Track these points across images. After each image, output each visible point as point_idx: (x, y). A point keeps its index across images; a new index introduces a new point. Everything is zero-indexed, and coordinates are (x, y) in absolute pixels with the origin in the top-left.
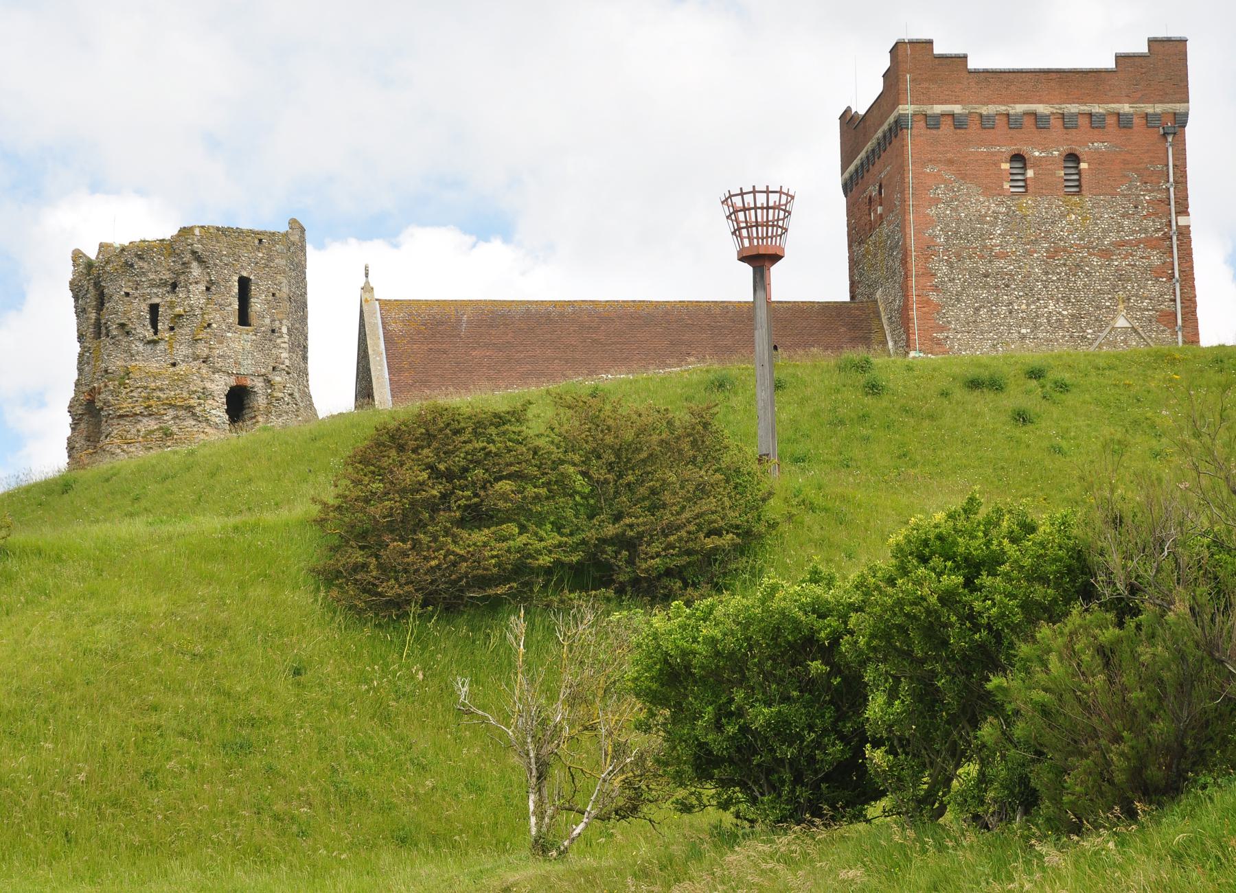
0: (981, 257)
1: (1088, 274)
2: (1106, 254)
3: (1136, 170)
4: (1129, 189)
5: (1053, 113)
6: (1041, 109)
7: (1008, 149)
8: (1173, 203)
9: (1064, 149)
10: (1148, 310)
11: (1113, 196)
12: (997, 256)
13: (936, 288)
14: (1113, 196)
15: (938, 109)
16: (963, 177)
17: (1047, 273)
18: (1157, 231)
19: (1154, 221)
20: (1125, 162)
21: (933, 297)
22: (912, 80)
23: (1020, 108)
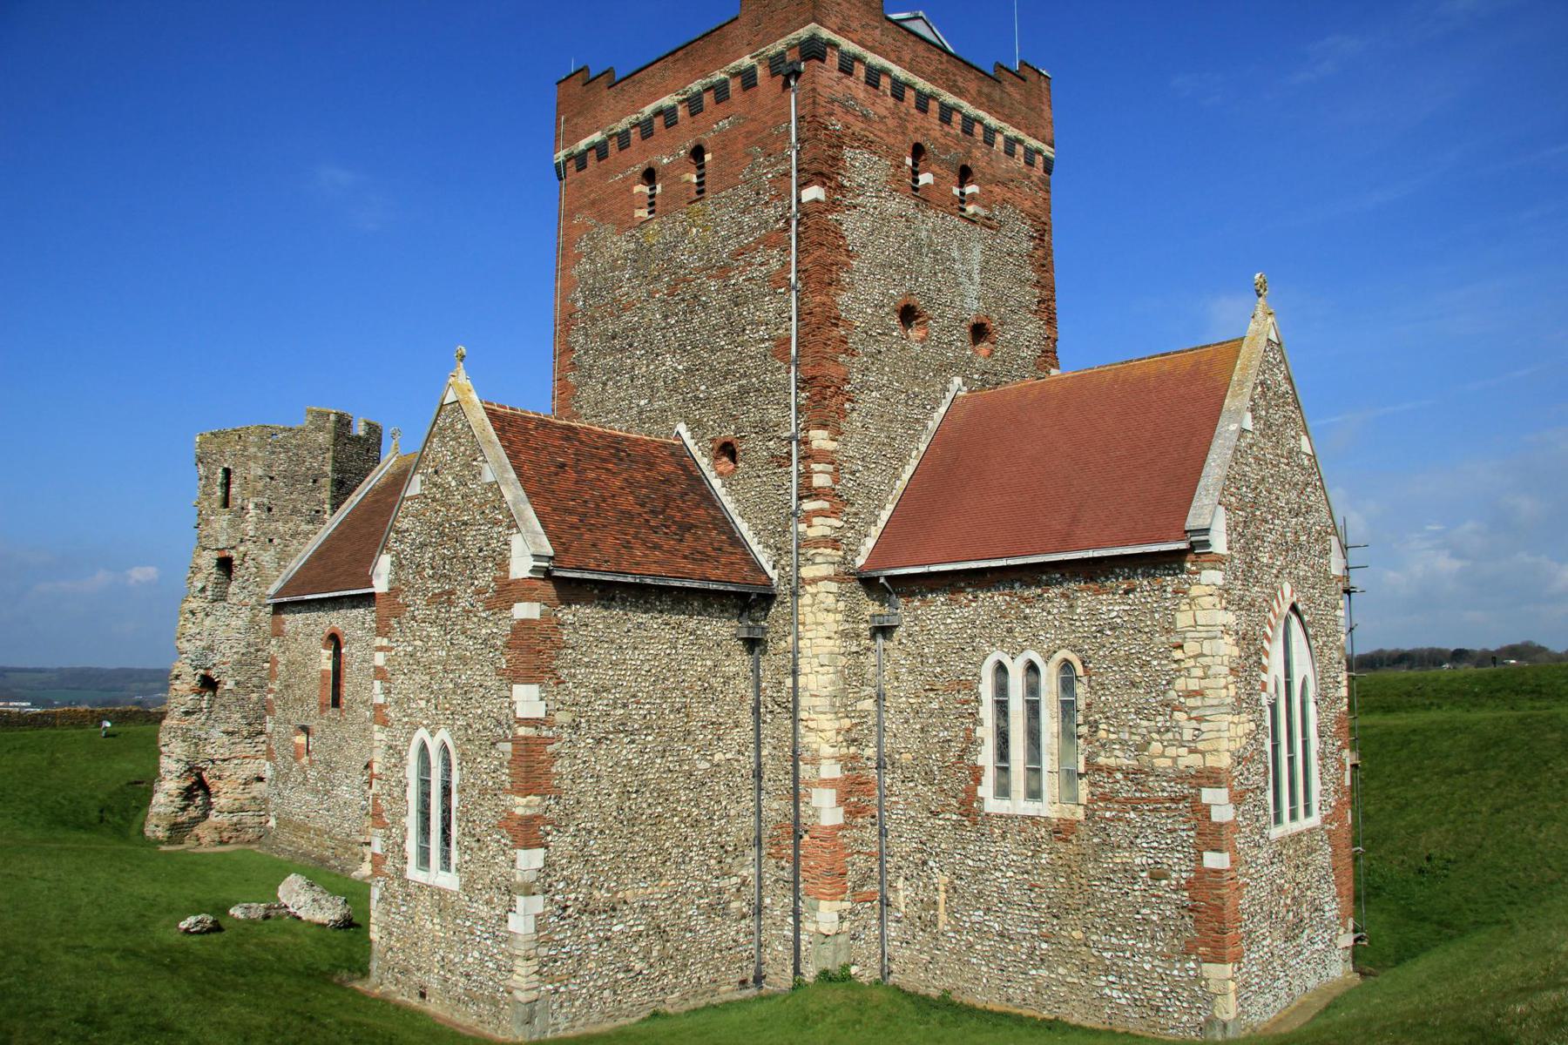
0: (611, 314)
1: (704, 306)
2: (724, 271)
3: (756, 143)
4: (752, 170)
5: (681, 102)
6: (667, 101)
7: (639, 168)
8: (794, 173)
9: (690, 144)
10: (763, 341)
11: (734, 187)
12: (624, 310)
13: (573, 366)
14: (734, 187)
15: (582, 145)
16: (602, 217)
17: (666, 317)
18: (777, 221)
19: (776, 207)
20: (749, 134)
21: (572, 378)
22: (566, 121)
23: (648, 110)
